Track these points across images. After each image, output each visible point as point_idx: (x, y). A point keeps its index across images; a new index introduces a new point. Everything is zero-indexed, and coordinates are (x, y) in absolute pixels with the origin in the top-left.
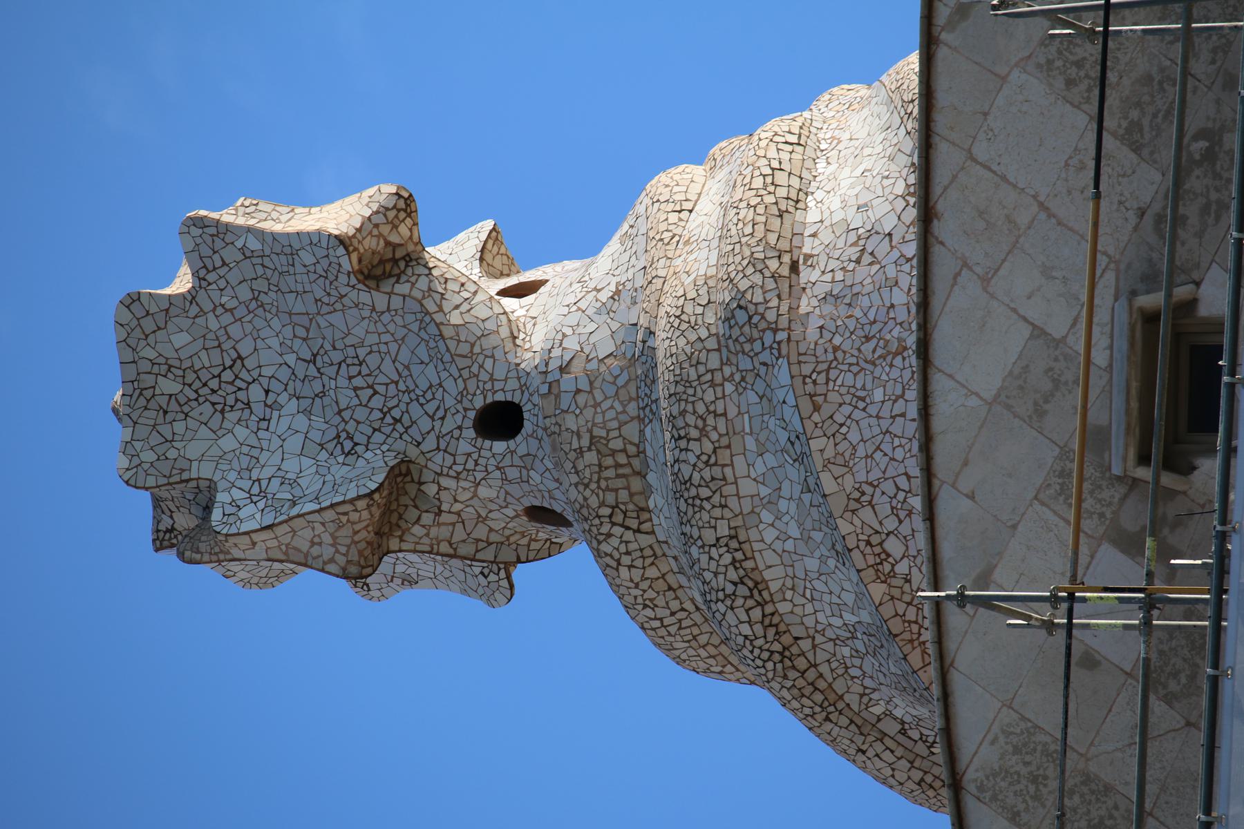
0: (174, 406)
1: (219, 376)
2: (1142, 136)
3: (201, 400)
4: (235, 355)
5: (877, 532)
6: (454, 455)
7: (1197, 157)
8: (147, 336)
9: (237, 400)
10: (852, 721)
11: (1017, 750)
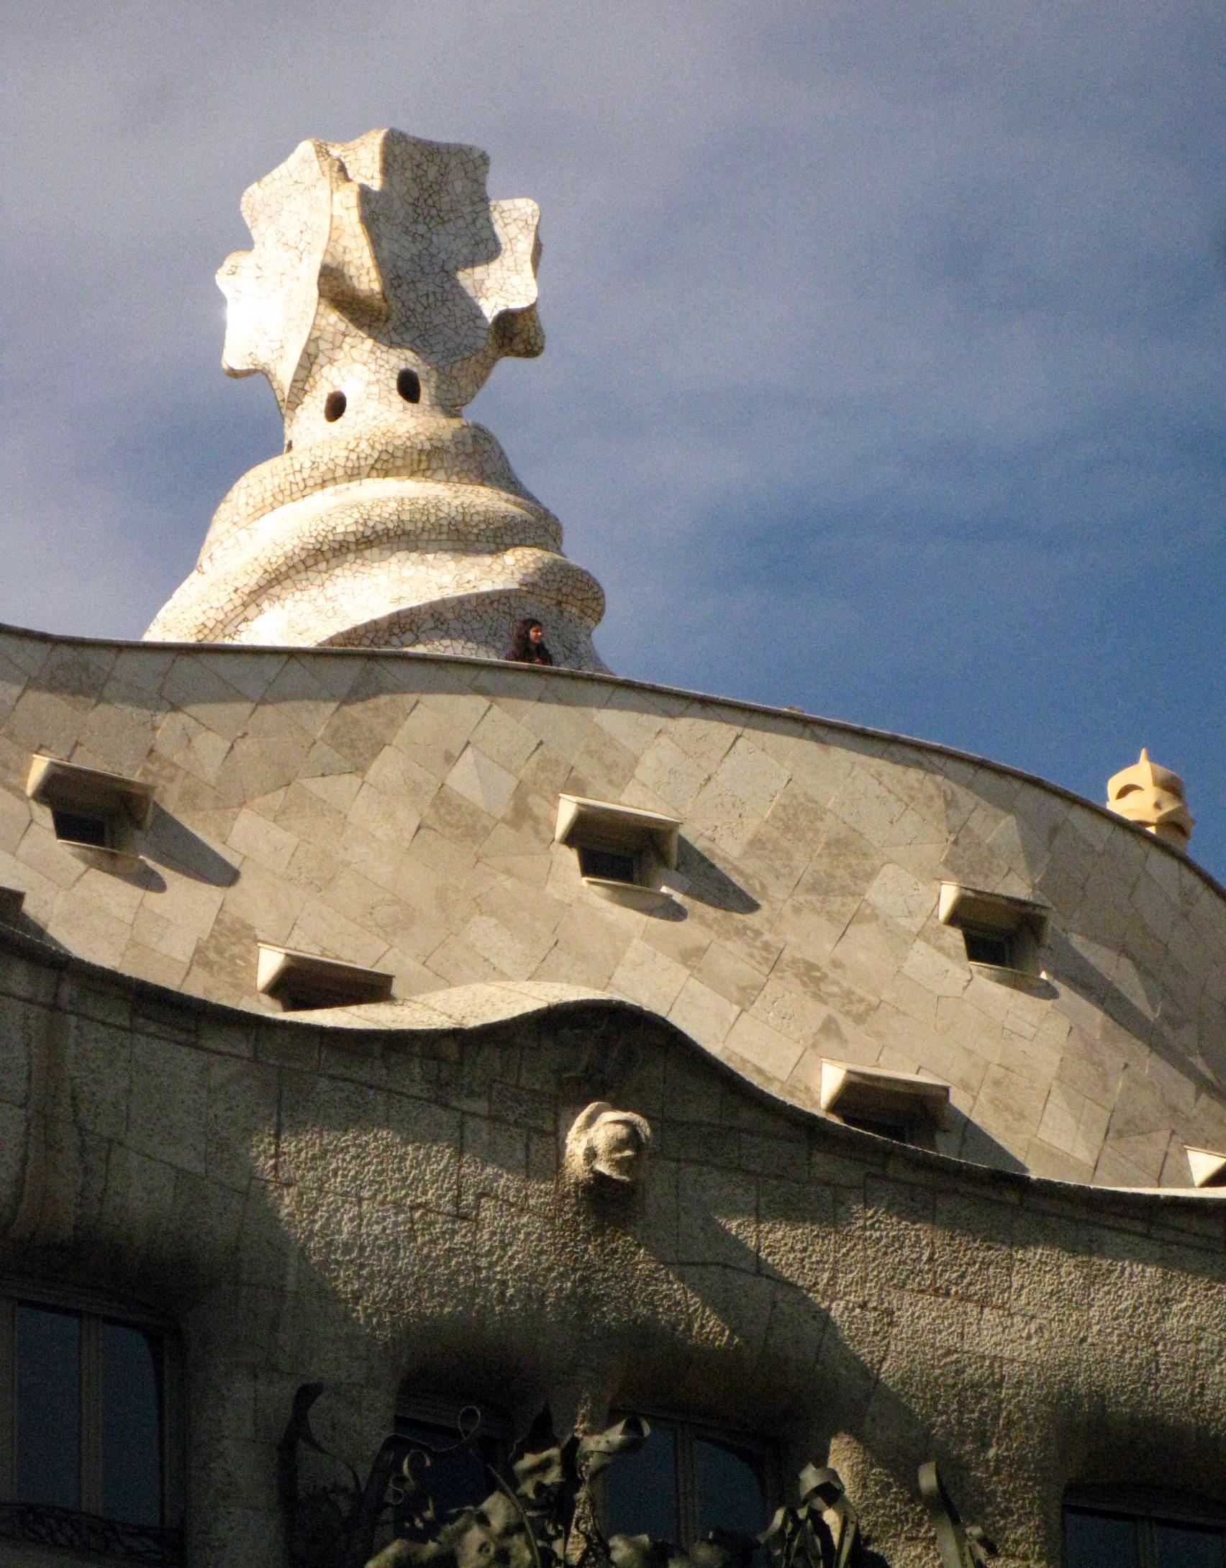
0: (421, 173)
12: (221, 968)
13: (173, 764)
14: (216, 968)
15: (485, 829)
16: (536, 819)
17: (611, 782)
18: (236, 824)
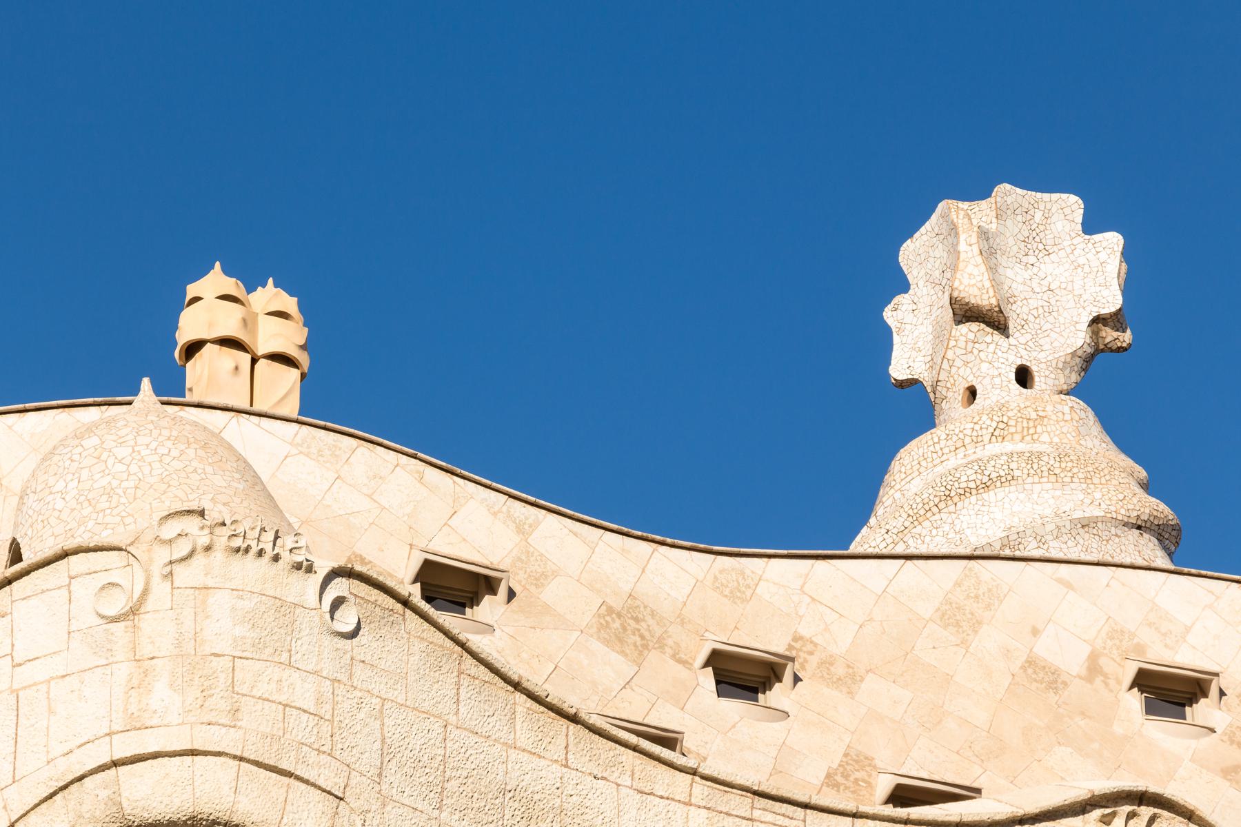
0: (1029, 217)
11: (990, 590)
12: (846, 788)
13: (812, 642)
14: (842, 788)
15: (1065, 683)
16: (1106, 676)
17: (1166, 646)
18: (863, 685)
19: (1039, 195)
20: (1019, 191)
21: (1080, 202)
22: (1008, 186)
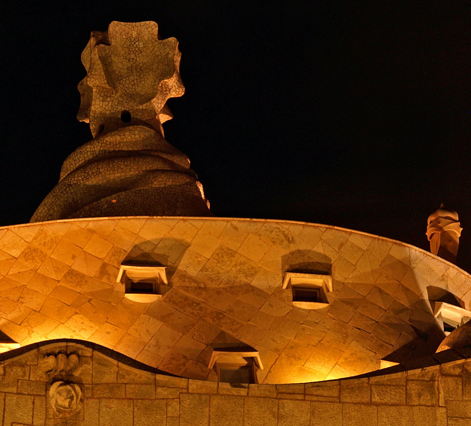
0: (130, 35)
1: (137, 47)
2: (205, 272)
3: (131, 42)
4: (142, 51)
5: (102, 208)
6: (117, 105)
7: (200, 285)
8: (147, 29)
9: (131, 51)
10: (53, 202)
11: (51, 239)
19: (134, 24)
20: (122, 23)
21: (156, 24)
22: (116, 22)
